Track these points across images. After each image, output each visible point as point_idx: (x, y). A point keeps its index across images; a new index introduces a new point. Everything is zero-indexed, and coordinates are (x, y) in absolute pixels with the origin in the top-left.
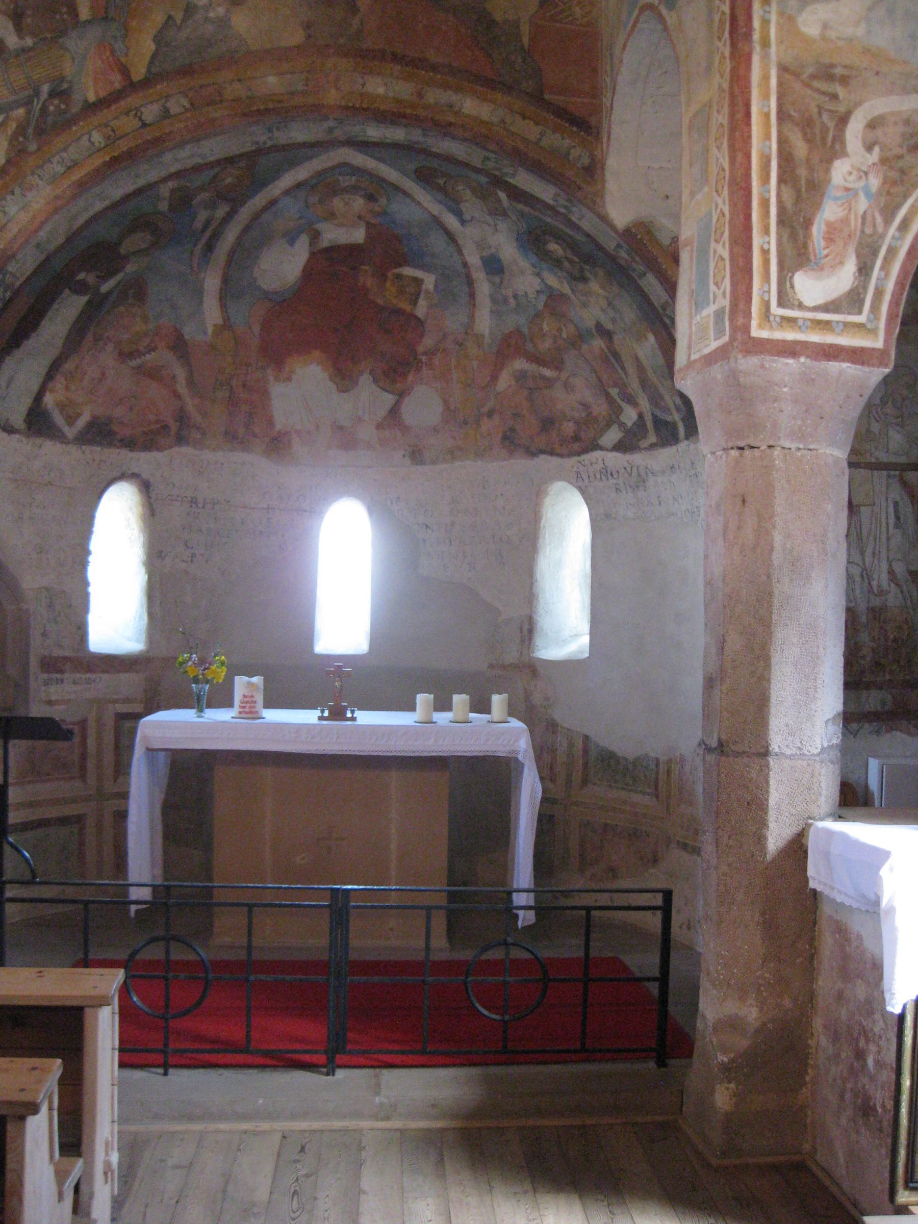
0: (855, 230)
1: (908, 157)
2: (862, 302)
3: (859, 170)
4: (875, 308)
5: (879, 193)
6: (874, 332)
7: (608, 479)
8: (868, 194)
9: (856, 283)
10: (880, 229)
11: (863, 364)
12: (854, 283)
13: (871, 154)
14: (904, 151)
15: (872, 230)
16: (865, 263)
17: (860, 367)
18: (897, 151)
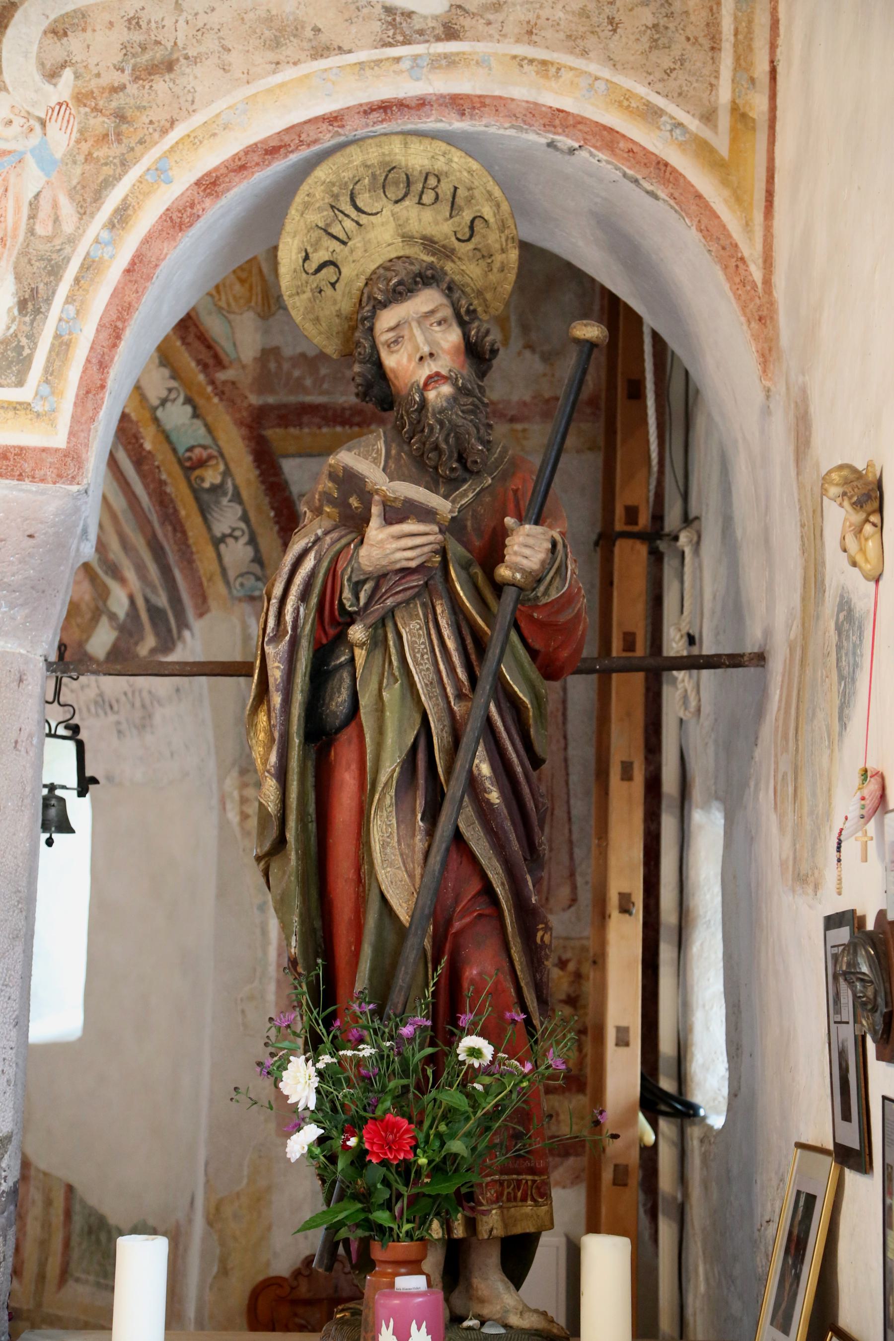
0: (15, 228)
1: (132, 89)
2: (25, 363)
3: (28, 116)
4: (52, 374)
5: (71, 158)
6: (48, 417)
7: (106, 713)
8: (44, 161)
9: (14, 327)
10: (68, 226)
11: (20, 477)
12: (9, 328)
13: (55, 85)
14: (125, 78)
15: (50, 228)
16: (34, 292)
17: (15, 482)
18: (118, 78)
